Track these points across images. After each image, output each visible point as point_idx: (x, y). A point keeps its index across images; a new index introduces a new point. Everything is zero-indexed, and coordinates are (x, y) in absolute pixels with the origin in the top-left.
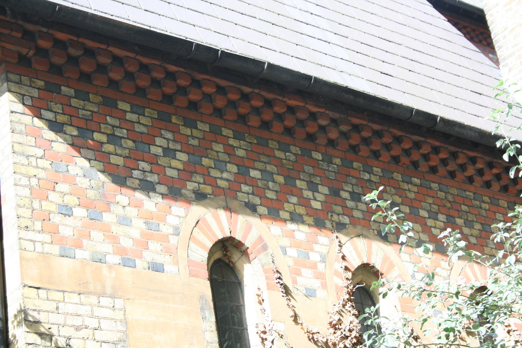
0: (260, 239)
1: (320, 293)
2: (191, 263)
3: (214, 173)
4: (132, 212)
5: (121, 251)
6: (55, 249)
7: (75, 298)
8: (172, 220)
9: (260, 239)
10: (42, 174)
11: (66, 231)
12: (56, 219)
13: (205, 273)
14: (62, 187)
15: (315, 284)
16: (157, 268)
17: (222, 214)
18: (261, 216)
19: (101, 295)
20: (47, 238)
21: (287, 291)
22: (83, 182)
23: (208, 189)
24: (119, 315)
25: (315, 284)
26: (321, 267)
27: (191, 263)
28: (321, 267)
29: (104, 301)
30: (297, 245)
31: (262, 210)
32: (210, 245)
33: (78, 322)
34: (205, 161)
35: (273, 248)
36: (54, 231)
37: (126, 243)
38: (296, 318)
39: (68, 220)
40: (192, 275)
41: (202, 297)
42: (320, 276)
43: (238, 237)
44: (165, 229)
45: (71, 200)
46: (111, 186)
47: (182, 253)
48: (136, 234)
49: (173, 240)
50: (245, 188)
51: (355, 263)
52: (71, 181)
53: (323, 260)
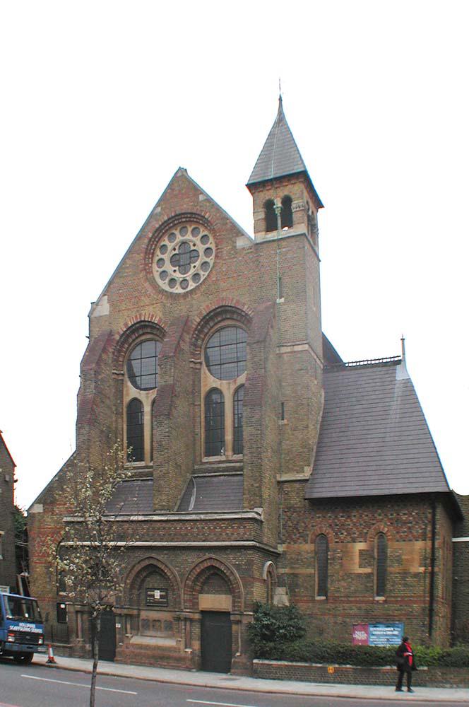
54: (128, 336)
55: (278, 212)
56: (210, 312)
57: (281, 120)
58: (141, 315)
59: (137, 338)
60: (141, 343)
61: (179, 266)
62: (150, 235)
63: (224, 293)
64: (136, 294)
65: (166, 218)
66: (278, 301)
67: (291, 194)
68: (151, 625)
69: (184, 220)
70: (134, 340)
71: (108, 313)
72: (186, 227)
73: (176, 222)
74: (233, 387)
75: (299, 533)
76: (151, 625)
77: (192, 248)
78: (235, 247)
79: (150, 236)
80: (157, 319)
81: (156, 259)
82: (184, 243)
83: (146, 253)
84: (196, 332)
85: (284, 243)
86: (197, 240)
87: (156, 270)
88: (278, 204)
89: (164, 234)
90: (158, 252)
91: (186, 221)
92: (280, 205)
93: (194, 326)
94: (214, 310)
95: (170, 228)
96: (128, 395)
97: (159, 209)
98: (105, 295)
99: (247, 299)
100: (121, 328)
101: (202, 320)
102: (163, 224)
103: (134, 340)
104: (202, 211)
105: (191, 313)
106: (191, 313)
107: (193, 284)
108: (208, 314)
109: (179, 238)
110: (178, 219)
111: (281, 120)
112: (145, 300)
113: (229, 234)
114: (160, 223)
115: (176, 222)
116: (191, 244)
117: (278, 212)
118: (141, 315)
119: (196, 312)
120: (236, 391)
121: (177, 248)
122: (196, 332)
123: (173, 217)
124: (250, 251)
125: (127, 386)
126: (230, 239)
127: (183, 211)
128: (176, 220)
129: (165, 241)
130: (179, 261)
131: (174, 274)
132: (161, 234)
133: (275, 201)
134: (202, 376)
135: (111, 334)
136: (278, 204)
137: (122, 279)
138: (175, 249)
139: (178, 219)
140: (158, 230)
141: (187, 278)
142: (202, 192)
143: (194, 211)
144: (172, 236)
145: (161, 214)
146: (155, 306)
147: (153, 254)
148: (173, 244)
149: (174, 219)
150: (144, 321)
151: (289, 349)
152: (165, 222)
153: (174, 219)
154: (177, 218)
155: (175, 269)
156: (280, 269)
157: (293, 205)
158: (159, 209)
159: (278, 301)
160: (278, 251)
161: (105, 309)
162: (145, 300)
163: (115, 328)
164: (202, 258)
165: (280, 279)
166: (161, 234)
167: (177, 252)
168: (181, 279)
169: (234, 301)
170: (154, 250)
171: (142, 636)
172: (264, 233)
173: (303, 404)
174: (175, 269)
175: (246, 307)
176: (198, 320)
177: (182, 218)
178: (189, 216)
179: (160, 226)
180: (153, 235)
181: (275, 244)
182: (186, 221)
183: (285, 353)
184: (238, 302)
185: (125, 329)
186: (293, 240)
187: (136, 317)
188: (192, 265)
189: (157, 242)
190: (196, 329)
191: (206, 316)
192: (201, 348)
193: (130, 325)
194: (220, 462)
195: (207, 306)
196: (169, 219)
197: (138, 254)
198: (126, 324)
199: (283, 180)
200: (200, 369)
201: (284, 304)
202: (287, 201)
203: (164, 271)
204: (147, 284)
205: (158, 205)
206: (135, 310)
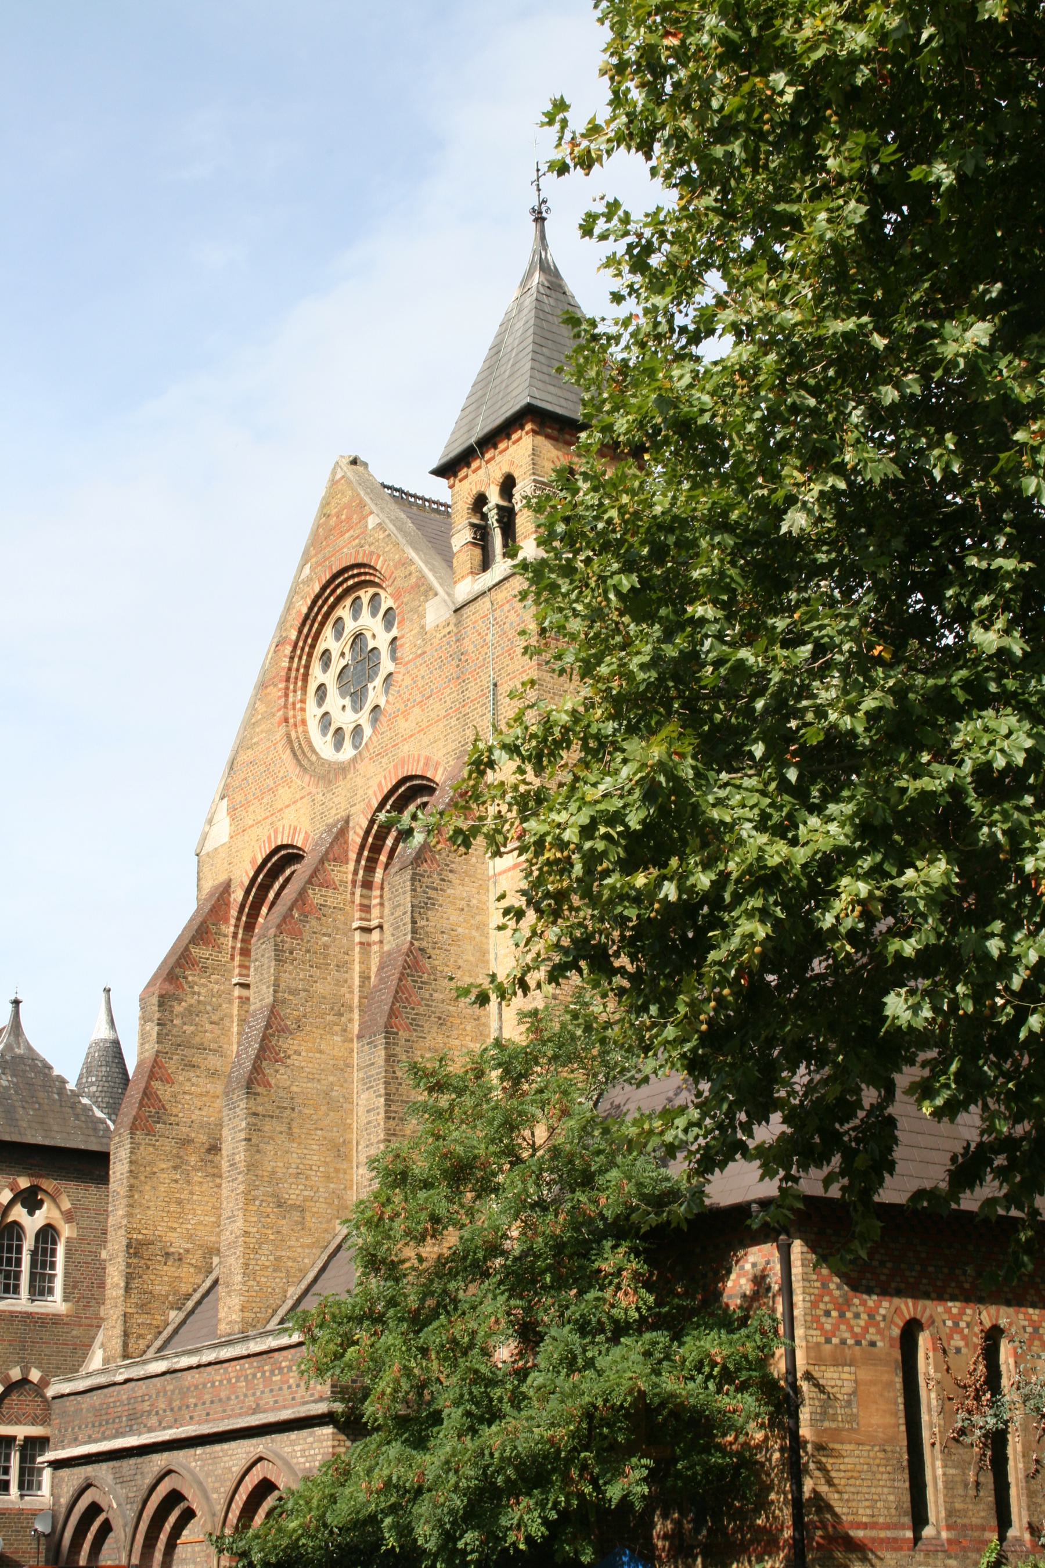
0: (931, 1316)
1: (964, 1350)
2: (891, 1338)
3: (907, 1273)
4: (861, 1309)
5: (854, 1335)
6: (822, 1340)
7: (832, 1369)
8: (882, 1311)
9: (931, 1316)
10: (816, 1291)
11: (828, 1327)
12: (823, 1319)
13: (898, 1344)
14: (826, 1299)
15: (961, 1344)
16: (873, 1344)
17: (910, 1302)
18: (933, 1300)
19: (844, 1365)
20: (818, 1332)
21: (945, 1351)
22: (837, 1293)
23: (903, 1286)
24: (853, 1377)
25: (961, 1344)
26: (966, 1331)
27: (891, 1338)
28: (966, 1331)
29: (847, 1369)
30: (952, 1317)
31: (933, 1295)
32: (901, 1324)
33: (833, 1383)
34: (903, 1266)
35: (938, 1322)
36: (821, 1327)
37: (857, 1330)
38: (948, 1370)
39: (830, 1320)
40: (892, 1346)
41: (896, 1361)
42: (964, 1338)
43: (918, 1317)
44: (879, 1318)
45: (830, 1306)
46: (851, 1293)
47: (886, 1333)
48: (862, 1323)
49: (882, 1325)
50: (924, 1281)
51: (988, 1324)
52: (830, 1293)
53: (968, 1325)
58: (276, 832)
63: (406, 748)
64: (270, 782)
69: (351, 582)
72: (358, 598)
73: (339, 591)
78: (423, 627)
79: (294, 637)
80: (302, 836)
81: (312, 687)
83: (288, 680)
87: (313, 711)
88: (494, 498)
89: (322, 624)
93: (359, 840)
95: (332, 607)
97: (307, 570)
100: (243, 873)
102: (314, 602)
104: (372, 553)
105: (353, 810)
106: (353, 810)
109: (350, 626)
112: (285, 794)
113: (414, 600)
114: (309, 602)
115: (339, 591)
116: (368, 635)
118: (276, 832)
121: (347, 650)
124: (448, 629)
126: (415, 610)
127: (344, 565)
129: (328, 641)
132: (316, 625)
135: (226, 888)
137: (250, 752)
138: (343, 654)
141: (359, 722)
143: (360, 561)
145: (309, 579)
147: (306, 675)
152: (318, 597)
157: (517, 493)
158: (307, 570)
161: (221, 832)
165: (495, 685)
166: (316, 625)
168: (352, 726)
169: (421, 764)
170: (307, 667)
172: (470, 578)
175: (440, 771)
177: (346, 580)
179: (311, 609)
180: (300, 632)
183: (504, 872)
184: (428, 759)
187: (269, 837)
188: (370, 686)
189: (313, 646)
193: (259, 861)
196: (324, 589)
197: (276, 685)
202: (508, 484)
203: (326, 714)
204: (287, 755)
205: (305, 559)
206: (269, 821)
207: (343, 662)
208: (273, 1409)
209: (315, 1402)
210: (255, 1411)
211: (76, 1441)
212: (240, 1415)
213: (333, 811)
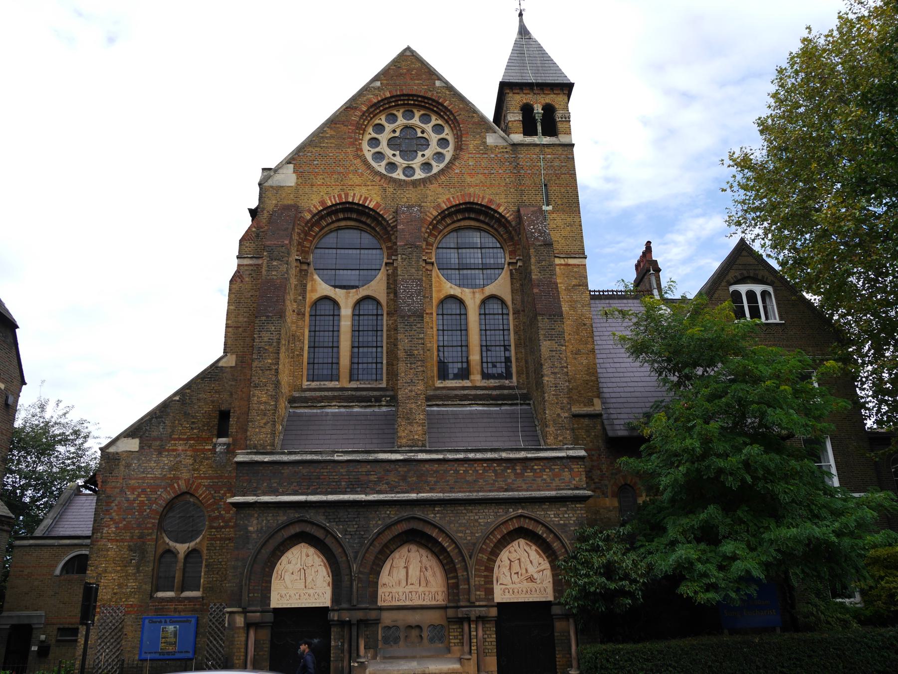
54: (322, 218)
55: (538, 117)
56: (453, 207)
57: (523, 32)
59: (333, 222)
60: (339, 229)
61: (400, 151)
62: (364, 109)
65: (388, 95)
66: (544, 208)
67: (554, 103)
68: (402, 636)
70: (328, 225)
71: (293, 184)
73: (399, 102)
74: (479, 297)
75: (594, 483)
76: (402, 636)
77: (420, 134)
78: (485, 143)
81: (367, 137)
82: (406, 127)
84: (431, 227)
85: (549, 150)
86: (428, 127)
88: (538, 109)
89: (380, 112)
90: (370, 130)
91: (414, 105)
92: (541, 111)
94: (456, 205)
96: (314, 290)
97: (378, 84)
98: (289, 162)
99: (503, 200)
101: (439, 214)
102: (382, 100)
103: (328, 225)
107: (421, 173)
108: (448, 209)
109: (401, 121)
110: (404, 100)
111: (523, 32)
114: (380, 99)
115: (399, 102)
116: (419, 131)
117: (538, 117)
119: (433, 205)
120: (484, 302)
122: (431, 227)
123: (397, 96)
125: (313, 280)
127: (414, 93)
128: (401, 100)
130: (400, 145)
131: (395, 158)
133: (535, 106)
134: (433, 279)
136: (538, 109)
137: (318, 149)
138: (394, 131)
139: (404, 100)
140: (375, 105)
141: (414, 166)
142: (439, 78)
143: (429, 95)
144: (392, 118)
146: (370, 187)
147: (364, 130)
148: (392, 126)
149: (398, 99)
150: (352, 203)
151: (562, 261)
152: (386, 99)
153: (398, 99)
154: (402, 98)
155: (394, 152)
156: (546, 175)
159: (544, 208)
160: (541, 156)
162: (356, 180)
163: (304, 203)
164: (434, 147)
165: (545, 185)
167: (397, 134)
168: (404, 166)
170: (366, 126)
171: (385, 658)
173: (585, 325)
174: (394, 152)
176: (435, 213)
177: (408, 100)
178: (420, 99)
179: (379, 102)
180: (368, 109)
181: (537, 150)
182: (414, 105)
184: (491, 201)
185: (321, 208)
186: (559, 148)
189: (371, 119)
190: (431, 223)
191: (446, 210)
192: (432, 246)
194: (464, 388)
195: (448, 199)
196: (392, 97)
198: (322, 202)
199: (545, 88)
200: (431, 271)
201: (552, 212)
205: (376, 78)
207: (393, 135)
208: (527, 490)
209: (572, 489)
210: (506, 490)
211: (276, 493)
212: (490, 491)
213: (405, 200)
